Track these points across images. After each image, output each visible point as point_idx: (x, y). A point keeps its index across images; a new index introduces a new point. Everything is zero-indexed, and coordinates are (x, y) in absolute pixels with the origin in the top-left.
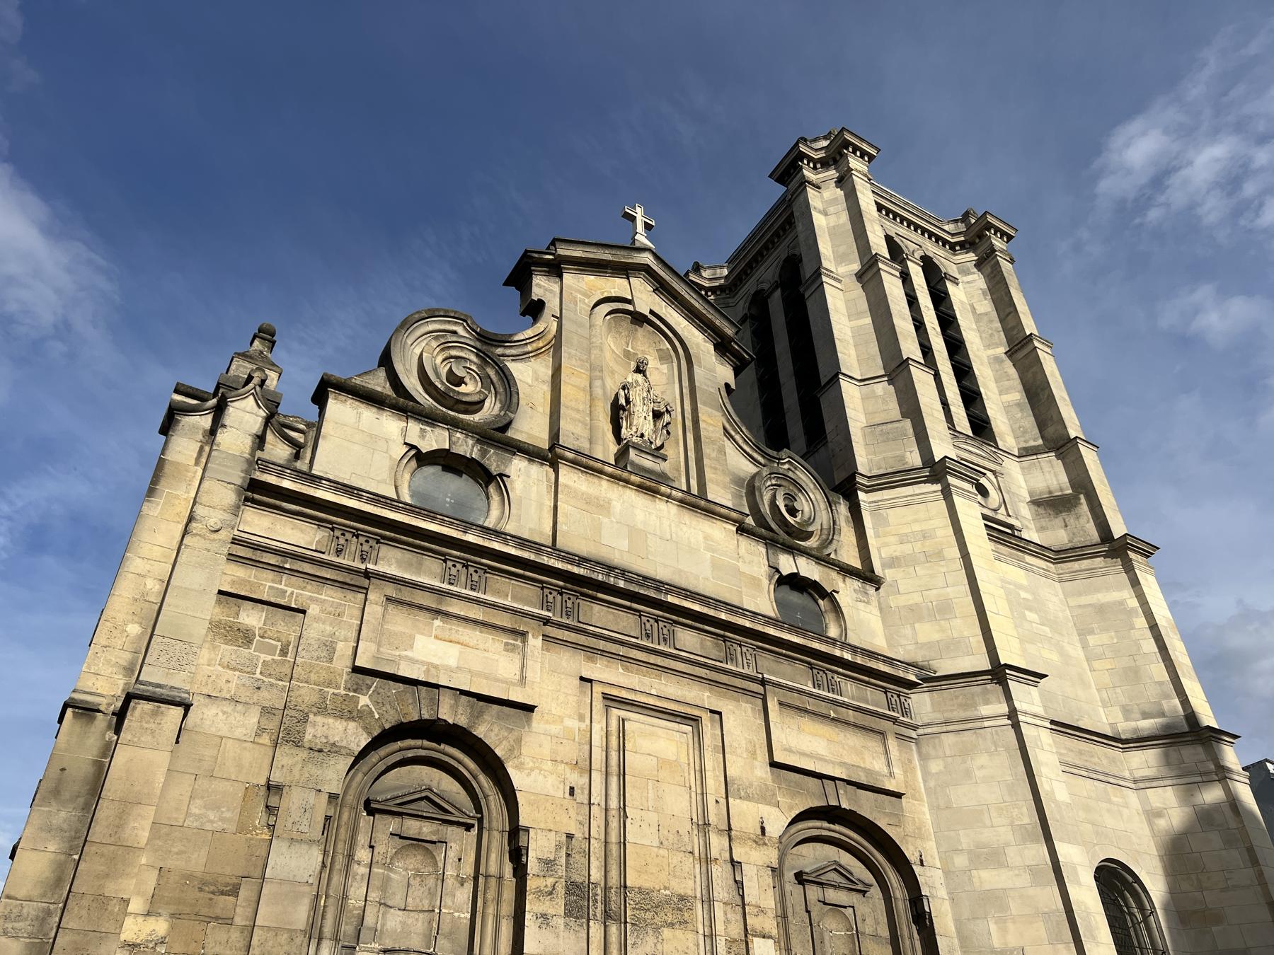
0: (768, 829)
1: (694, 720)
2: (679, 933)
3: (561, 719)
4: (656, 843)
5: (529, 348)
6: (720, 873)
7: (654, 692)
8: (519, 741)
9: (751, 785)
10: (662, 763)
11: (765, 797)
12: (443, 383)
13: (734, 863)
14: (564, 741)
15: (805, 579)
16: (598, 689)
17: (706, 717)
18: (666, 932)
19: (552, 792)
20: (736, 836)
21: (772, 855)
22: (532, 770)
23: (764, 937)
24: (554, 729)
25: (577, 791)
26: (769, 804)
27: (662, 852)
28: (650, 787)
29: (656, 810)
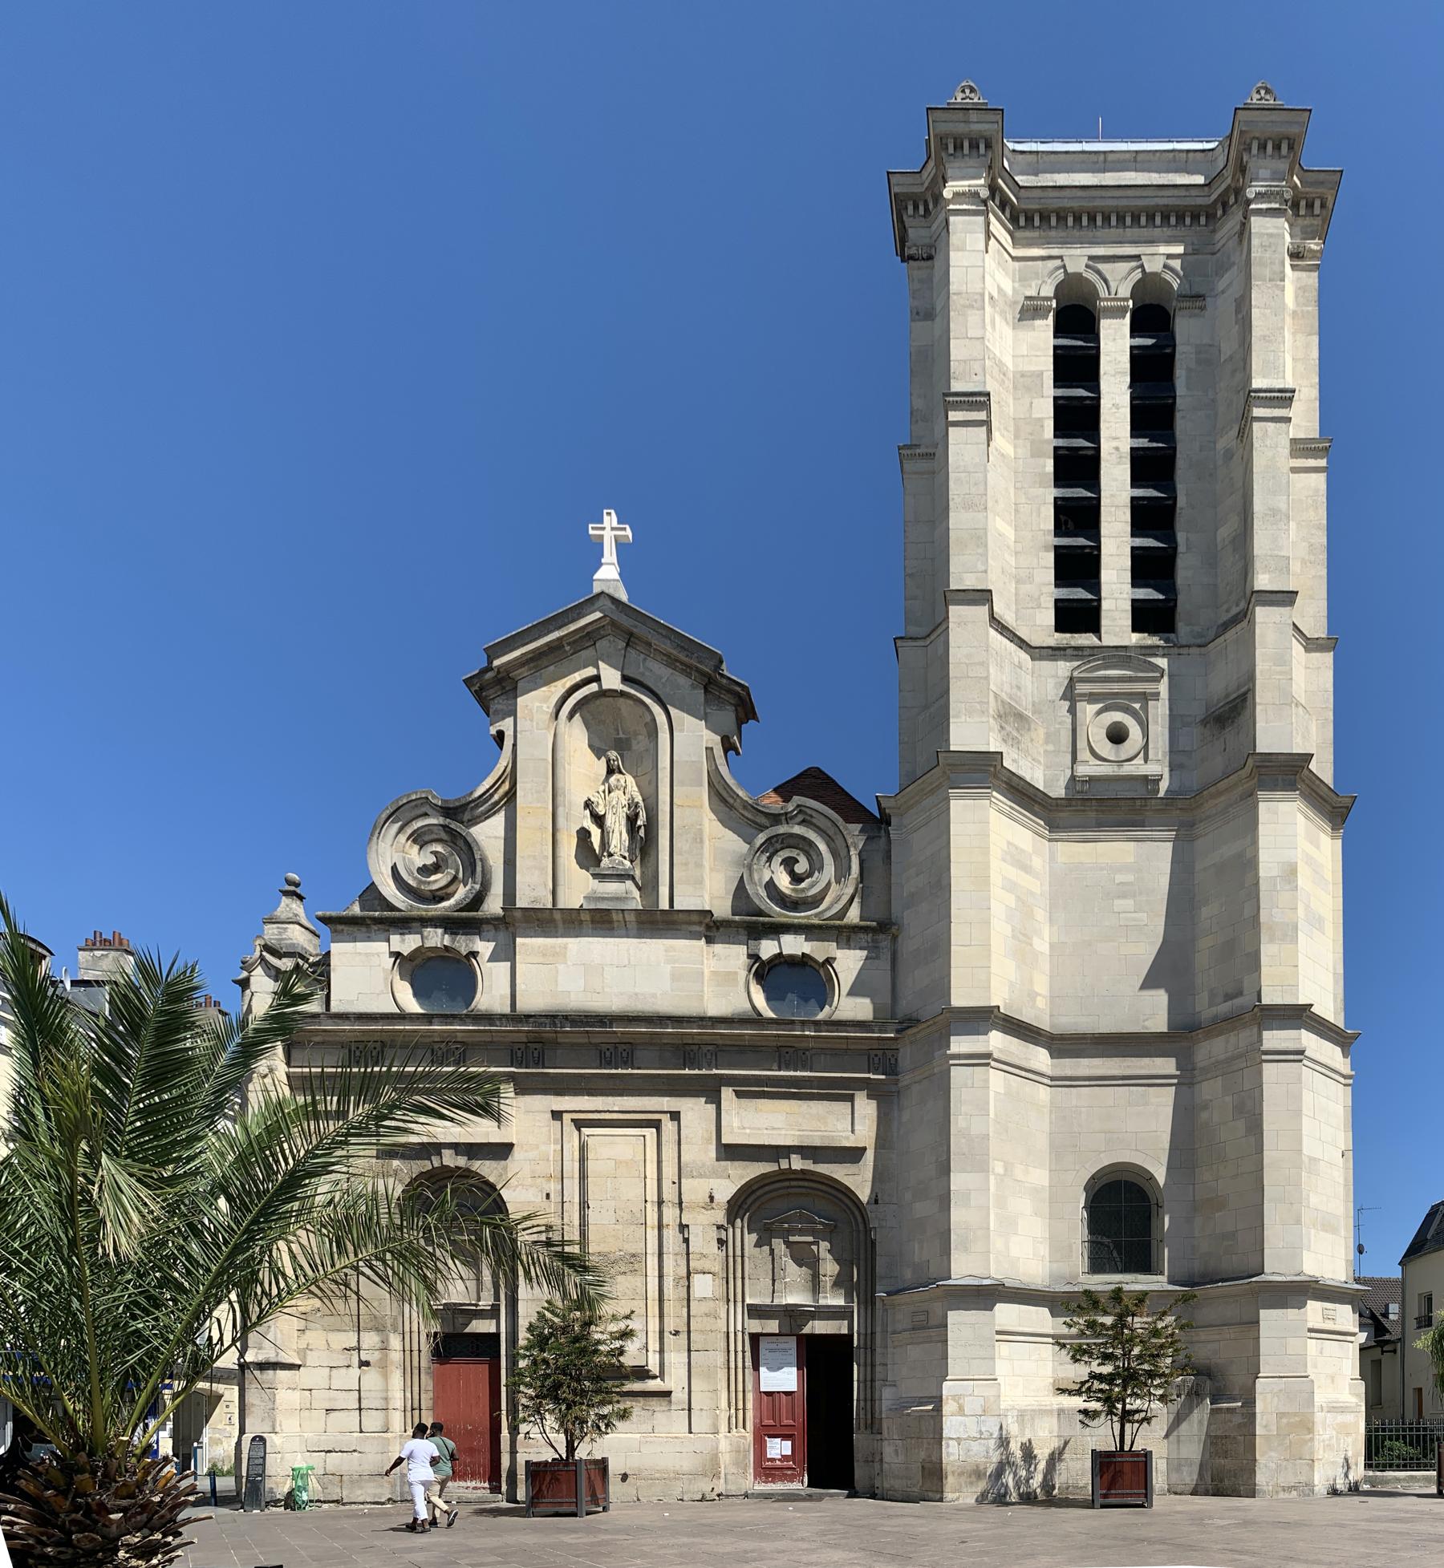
0: (716, 1197)
1: (656, 1125)
2: (629, 1278)
3: (537, 1147)
4: (614, 1221)
5: (496, 797)
6: (672, 1236)
7: (616, 1109)
8: (505, 1169)
9: (704, 1165)
10: (618, 1163)
11: (715, 1174)
12: (415, 878)
13: (683, 1228)
14: (540, 1162)
15: (792, 957)
16: (567, 1117)
17: (665, 1118)
18: (620, 1278)
19: (533, 1199)
20: (687, 1207)
21: (720, 1217)
22: (517, 1186)
23: (704, 1273)
24: (533, 1154)
25: (552, 1196)
26: (721, 1177)
27: (617, 1226)
28: (609, 1184)
29: (614, 1198)
